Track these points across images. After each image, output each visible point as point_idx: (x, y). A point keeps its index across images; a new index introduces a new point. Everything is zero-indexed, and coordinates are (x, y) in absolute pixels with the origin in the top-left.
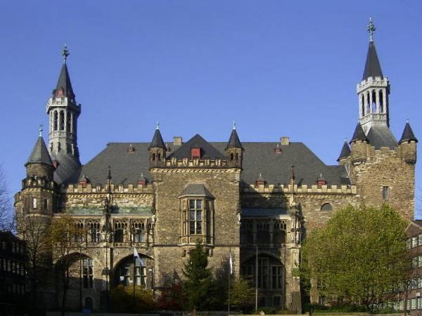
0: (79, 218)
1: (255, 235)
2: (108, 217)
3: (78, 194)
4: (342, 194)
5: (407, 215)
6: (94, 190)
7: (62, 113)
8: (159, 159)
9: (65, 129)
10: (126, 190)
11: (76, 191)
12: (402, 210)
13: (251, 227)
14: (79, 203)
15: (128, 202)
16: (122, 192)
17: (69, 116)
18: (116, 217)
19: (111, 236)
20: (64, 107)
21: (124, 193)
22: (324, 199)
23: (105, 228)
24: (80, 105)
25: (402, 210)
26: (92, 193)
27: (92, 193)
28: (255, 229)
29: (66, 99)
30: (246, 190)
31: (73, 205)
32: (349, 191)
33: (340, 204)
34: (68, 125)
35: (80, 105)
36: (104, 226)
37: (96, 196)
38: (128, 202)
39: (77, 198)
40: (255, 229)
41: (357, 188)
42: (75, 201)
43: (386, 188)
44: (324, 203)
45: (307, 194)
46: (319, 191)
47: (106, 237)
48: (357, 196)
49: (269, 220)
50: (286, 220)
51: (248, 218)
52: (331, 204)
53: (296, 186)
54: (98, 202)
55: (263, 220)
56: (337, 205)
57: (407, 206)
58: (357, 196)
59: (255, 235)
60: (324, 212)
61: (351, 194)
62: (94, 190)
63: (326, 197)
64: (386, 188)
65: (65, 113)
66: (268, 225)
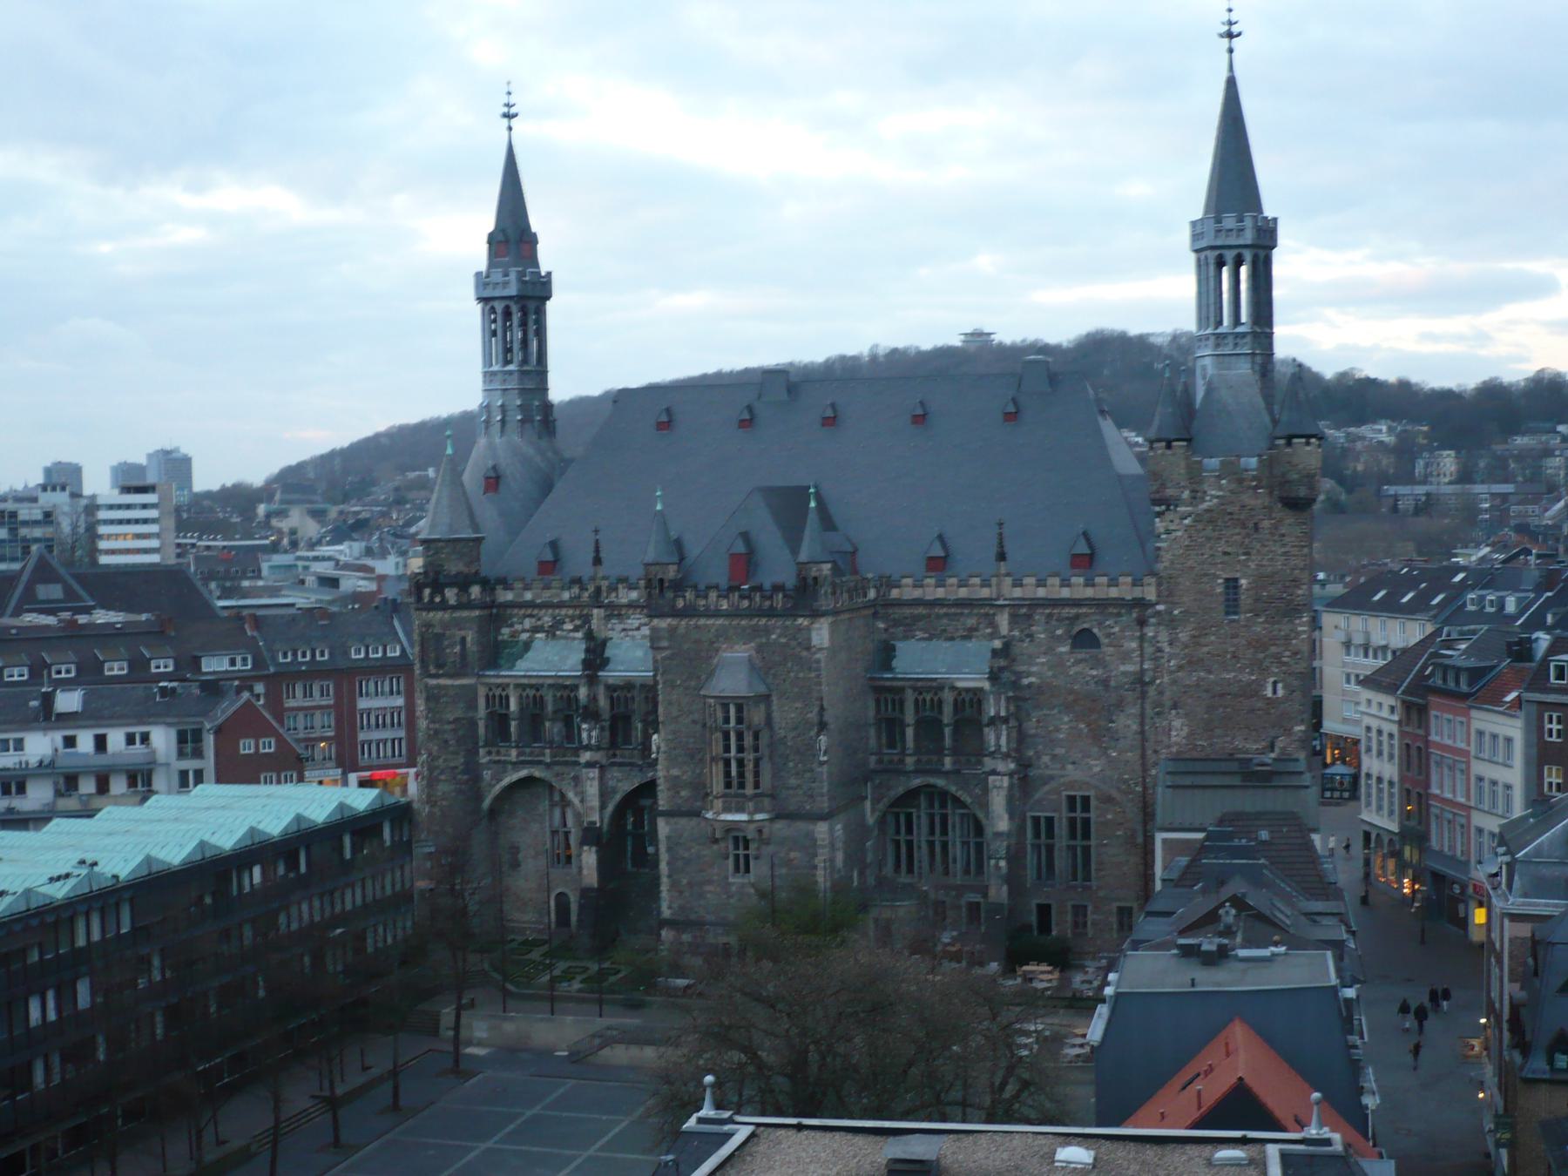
0: (533, 681)
1: (910, 732)
2: (592, 680)
3: (531, 605)
4: (1119, 603)
5: (1285, 664)
6: (566, 596)
7: (507, 314)
8: (661, 590)
9: (518, 355)
10: (634, 595)
11: (528, 596)
12: (1273, 649)
13: (902, 711)
14: (535, 630)
15: (638, 629)
16: (624, 601)
17: (525, 314)
18: (611, 681)
19: (602, 729)
20: (510, 298)
21: (632, 605)
22: (1077, 617)
23: (591, 714)
24: (549, 274)
25: (1273, 649)
26: (561, 605)
27: (561, 605)
28: (910, 717)
29: (513, 277)
30: (895, 593)
31: (525, 636)
32: (1138, 592)
33: (1116, 629)
34: (525, 343)
35: (549, 274)
36: (585, 708)
37: (571, 612)
38: (638, 629)
39: (531, 616)
40: (910, 717)
41: (1159, 585)
42: (528, 623)
43: (1232, 584)
44: (1077, 629)
45: (1036, 604)
46: (1065, 593)
47: (590, 737)
48: (1160, 607)
49: (941, 688)
50: (981, 690)
51: (895, 684)
52: (1095, 630)
53: (1009, 580)
54: (576, 629)
55: (929, 689)
56: (1108, 635)
57: (1287, 638)
58: (1160, 607)
59: (910, 732)
60: (1079, 656)
61: (1140, 603)
62: (566, 596)
63: (1084, 610)
64: (1232, 584)
65: (514, 308)
66: (940, 702)
